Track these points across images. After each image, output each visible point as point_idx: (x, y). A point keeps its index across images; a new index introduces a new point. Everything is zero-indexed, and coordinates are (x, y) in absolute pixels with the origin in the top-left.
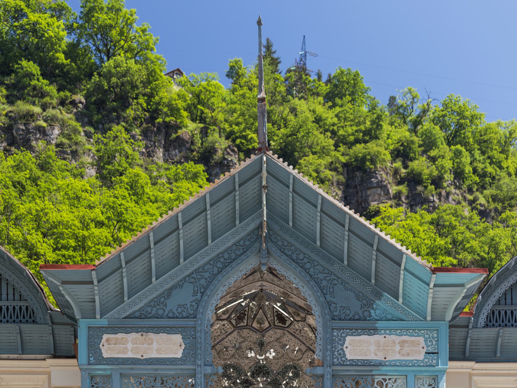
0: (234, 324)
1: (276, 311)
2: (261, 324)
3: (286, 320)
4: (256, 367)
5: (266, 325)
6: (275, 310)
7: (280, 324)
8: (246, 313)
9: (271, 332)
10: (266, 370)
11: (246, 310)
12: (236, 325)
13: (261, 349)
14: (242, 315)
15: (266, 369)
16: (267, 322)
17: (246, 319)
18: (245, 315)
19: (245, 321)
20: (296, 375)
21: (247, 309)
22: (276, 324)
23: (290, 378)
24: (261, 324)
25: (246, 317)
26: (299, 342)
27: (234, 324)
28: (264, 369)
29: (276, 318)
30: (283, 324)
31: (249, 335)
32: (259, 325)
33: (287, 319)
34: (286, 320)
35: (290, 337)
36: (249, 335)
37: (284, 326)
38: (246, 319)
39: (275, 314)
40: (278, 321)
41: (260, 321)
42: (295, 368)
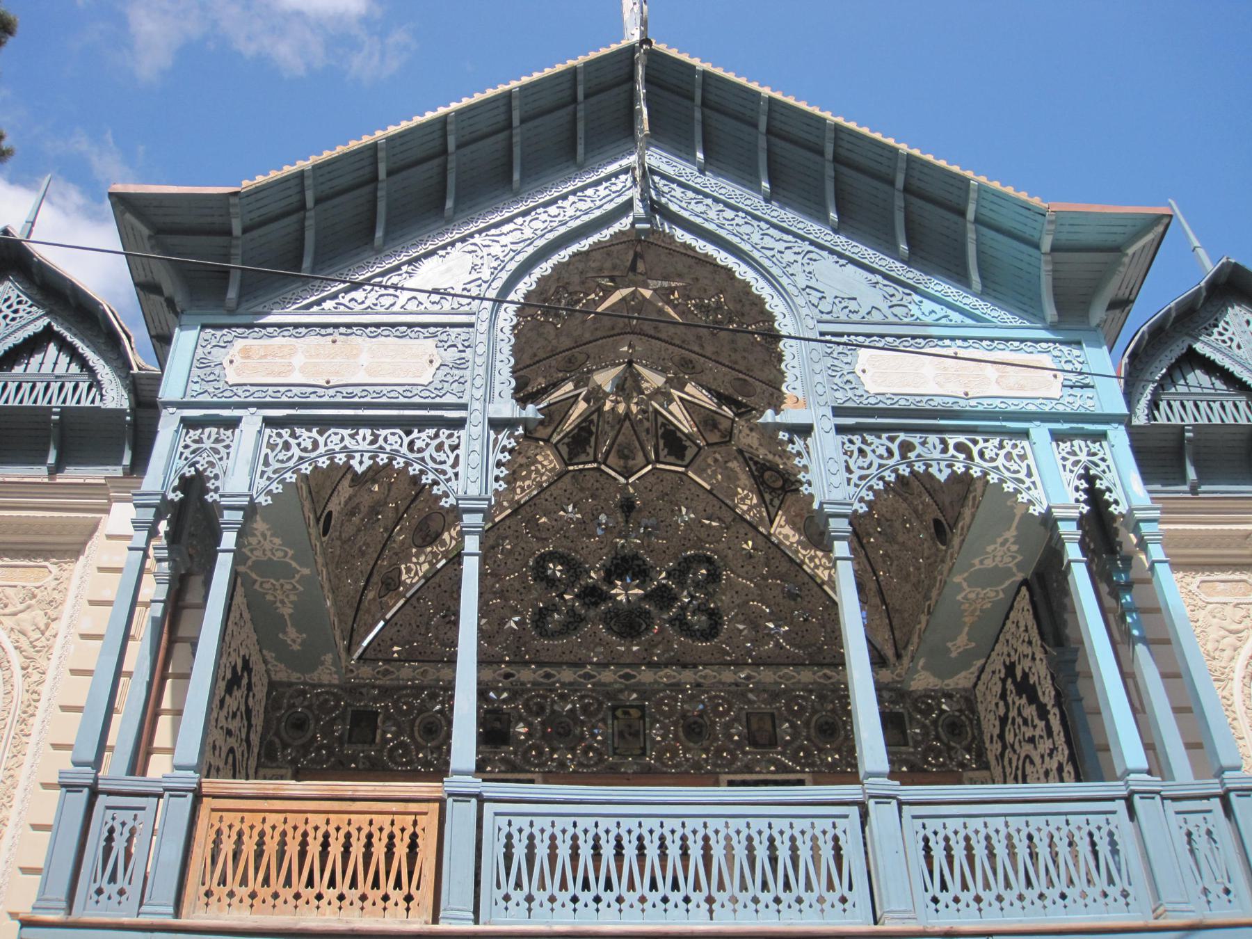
0: (566, 457)
1: (663, 425)
2: (626, 458)
3: (685, 448)
4: (615, 558)
6: (660, 420)
7: (671, 459)
8: (594, 429)
10: (639, 566)
11: (592, 421)
12: (570, 459)
13: (627, 517)
14: (584, 434)
15: (640, 562)
16: (640, 454)
17: (592, 443)
18: (591, 433)
19: (591, 451)
21: (595, 417)
22: (662, 459)
24: (626, 458)
25: (593, 439)
26: (716, 502)
27: (566, 457)
28: (636, 562)
29: (661, 442)
30: (678, 458)
31: (597, 485)
32: (622, 462)
33: (688, 443)
34: (685, 448)
36: (597, 485)
37: (679, 462)
38: (592, 443)
39: (660, 432)
40: (666, 451)
41: (626, 452)
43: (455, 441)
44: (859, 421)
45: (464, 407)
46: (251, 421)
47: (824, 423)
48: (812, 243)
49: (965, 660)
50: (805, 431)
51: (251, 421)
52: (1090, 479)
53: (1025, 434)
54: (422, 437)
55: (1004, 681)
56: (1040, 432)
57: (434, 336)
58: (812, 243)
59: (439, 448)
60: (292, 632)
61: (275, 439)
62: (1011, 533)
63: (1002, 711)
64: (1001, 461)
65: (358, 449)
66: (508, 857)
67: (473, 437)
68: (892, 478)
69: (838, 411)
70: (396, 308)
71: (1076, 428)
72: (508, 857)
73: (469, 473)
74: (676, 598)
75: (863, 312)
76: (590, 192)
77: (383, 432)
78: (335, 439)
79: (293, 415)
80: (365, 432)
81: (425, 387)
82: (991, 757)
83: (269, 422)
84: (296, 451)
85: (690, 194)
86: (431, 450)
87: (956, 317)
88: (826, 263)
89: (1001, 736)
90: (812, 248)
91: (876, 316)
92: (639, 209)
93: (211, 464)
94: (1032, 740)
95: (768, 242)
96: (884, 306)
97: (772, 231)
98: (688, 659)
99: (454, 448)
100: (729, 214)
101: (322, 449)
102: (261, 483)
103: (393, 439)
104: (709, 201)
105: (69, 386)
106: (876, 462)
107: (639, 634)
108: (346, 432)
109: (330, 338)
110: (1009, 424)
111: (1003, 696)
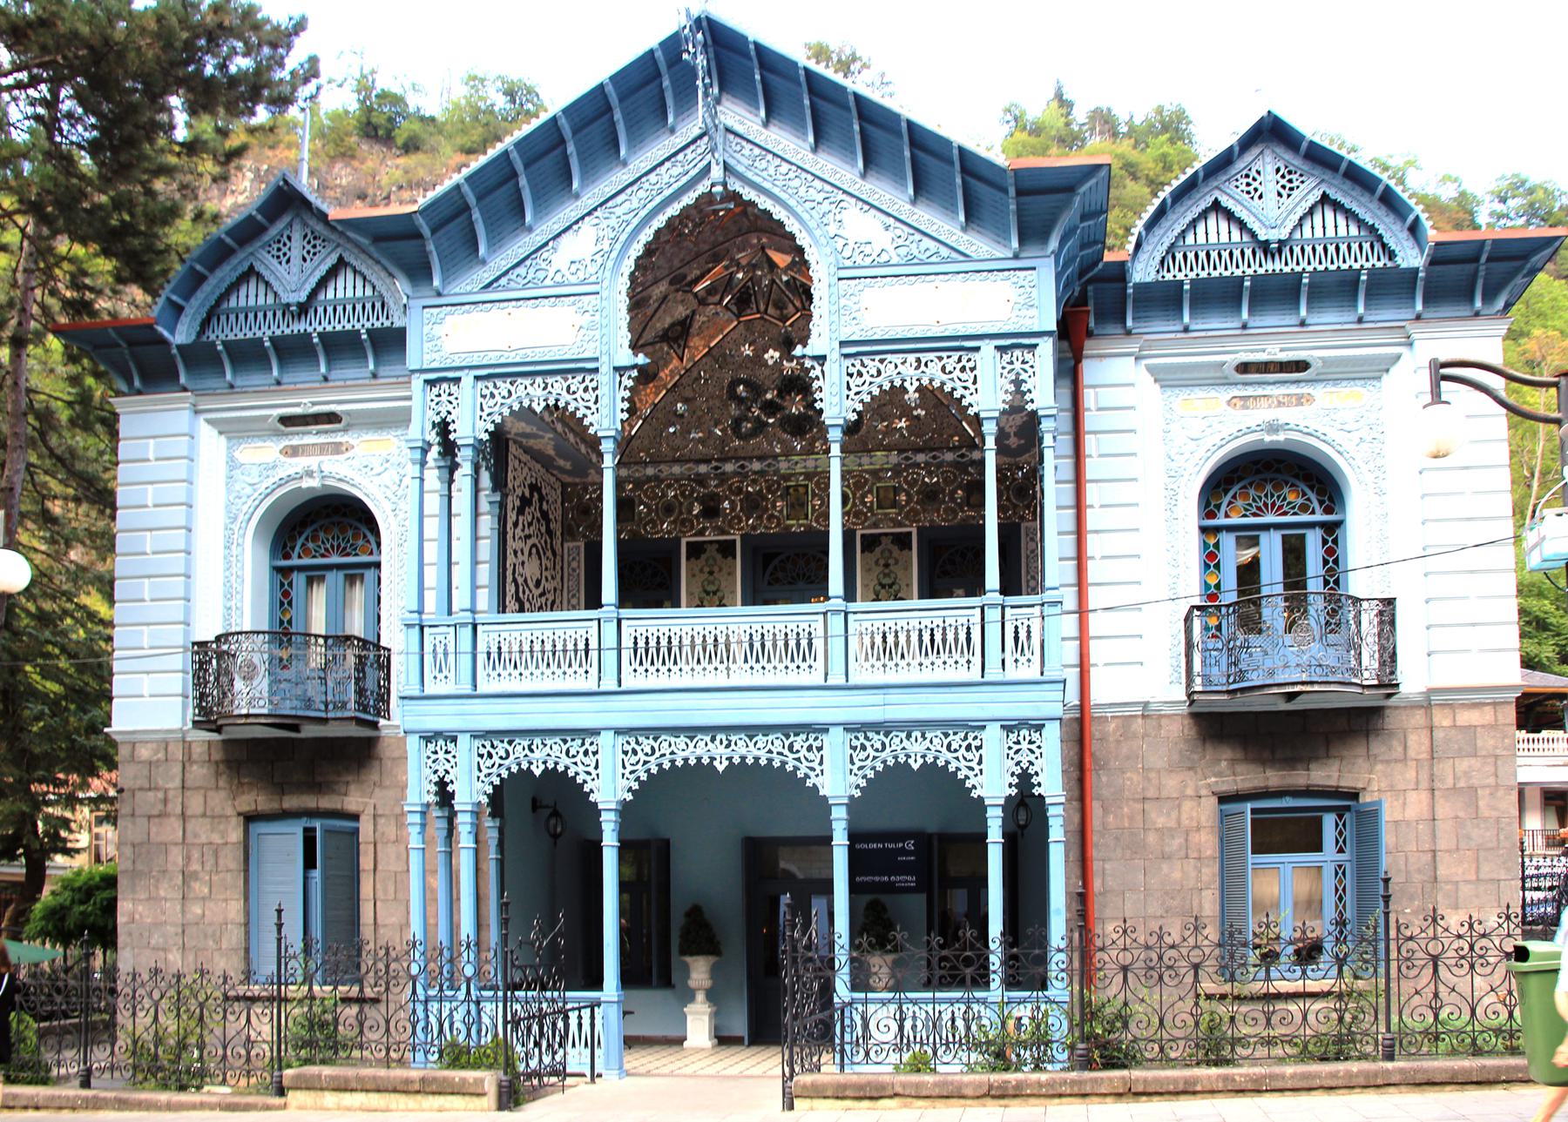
44: (858, 349)
47: (834, 356)
48: (845, 192)
50: (821, 359)
51: (467, 378)
58: (845, 192)
69: (843, 344)
73: (606, 415)
75: (874, 256)
77: (550, 380)
80: (539, 380)
83: (477, 378)
84: (498, 398)
85: (757, 151)
86: (581, 392)
87: (944, 252)
88: (852, 211)
90: (844, 197)
92: (717, 173)
95: (813, 194)
96: (890, 248)
97: (818, 184)
100: (785, 167)
102: (481, 425)
103: (558, 385)
104: (770, 157)
108: (527, 382)
110: (962, 345)
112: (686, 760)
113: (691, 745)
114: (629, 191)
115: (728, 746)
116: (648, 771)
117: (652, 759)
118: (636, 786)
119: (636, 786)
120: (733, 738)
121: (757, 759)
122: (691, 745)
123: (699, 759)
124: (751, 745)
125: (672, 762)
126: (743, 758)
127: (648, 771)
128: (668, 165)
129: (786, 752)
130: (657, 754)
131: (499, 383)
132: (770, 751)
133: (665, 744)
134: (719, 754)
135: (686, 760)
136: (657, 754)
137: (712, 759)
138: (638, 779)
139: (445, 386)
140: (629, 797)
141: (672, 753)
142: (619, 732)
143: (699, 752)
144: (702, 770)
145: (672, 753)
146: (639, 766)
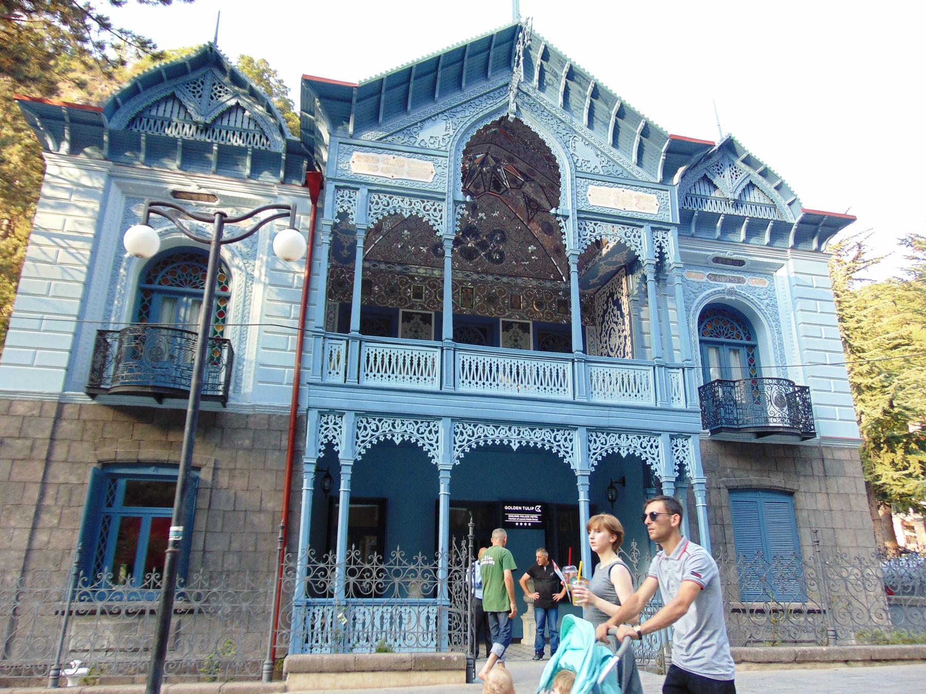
5: (482, 189)
9: (485, 197)
20: (503, 239)
23: (497, 242)
35: (502, 204)
42: (503, 232)
43: (440, 208)
44: (585, 216)
45: (444, 194)
46: (364, 191)
49: (594, 285)
50: (566, 217)
52: (660, 247)
53: (641, 227)
54: (429, 205)
55: (608, 298)
56: (647, 227)
57: (432, 160)
59: (435, 210)
60: (345, 251)
61: (372, 199)
62: (625, 253)
63: (605, 307)
64: (632, 238)
65: (405, 207)
66: (463, 368)
67: (446, 208)
68: (594, 240)
70: (416, 145)
71: (658, 226)
72: (463, 368)
74: (488, 246)
75: (592, 169)
76: (491, 94)
77: (414, 201)
78: (396, 201)
79: (376, 189)
80: (407, 199)
81: (430, 184)
82: (597, 322)
89: (603, 316)
91: (596, 171)
93: (349, 208)
94: (616, 323)
96: (600, 167)
98: (491, 271)
99: (440, 211)
101: (391, 206)
103: (418, 205)
105: (251, 135)
106: (590, 233)
107: (473, 259)
108: (400, 199)
109: (392, 156)
111: (607, 302)
112: (494, 441)
113: (497, 432)
114: (464, 106)
115: (519, 435)
116: (470, 446)
117: (473, 439)
118: (462, 456)
119: (462, 456)
120: (522, 430)
121: (536, 443)
122: (497, 432)
123: (502, 441)
124: (532, 434)
125: (485, 441)
126: (528, 442)
127: (470, 446)
128: (485, 97)
129: (552, 441)
130: (476, 436)
131: (382, 196)
132: (543, 440)
133: (480, 431)
134: (514, 438)
135: (494, 441)
136: (476, 436)
137: (510, 442)
138: (463, 451)
139: (347, 191)
140: (458, 463)
141: (485, 436)
142: (454, 419)
143: (501, 436)
144: (503, 449)
145: (485, 436)
146: (464, 443)
